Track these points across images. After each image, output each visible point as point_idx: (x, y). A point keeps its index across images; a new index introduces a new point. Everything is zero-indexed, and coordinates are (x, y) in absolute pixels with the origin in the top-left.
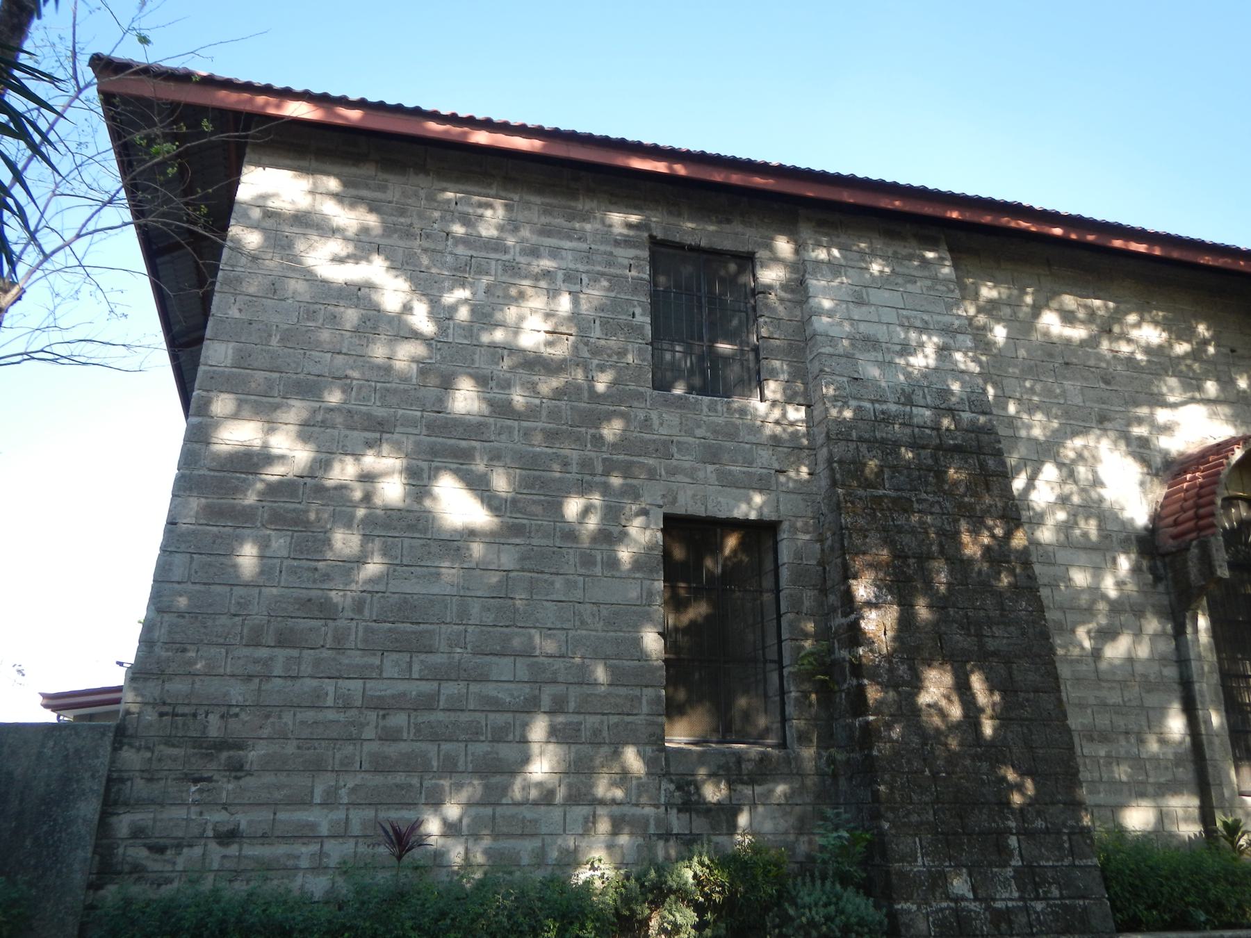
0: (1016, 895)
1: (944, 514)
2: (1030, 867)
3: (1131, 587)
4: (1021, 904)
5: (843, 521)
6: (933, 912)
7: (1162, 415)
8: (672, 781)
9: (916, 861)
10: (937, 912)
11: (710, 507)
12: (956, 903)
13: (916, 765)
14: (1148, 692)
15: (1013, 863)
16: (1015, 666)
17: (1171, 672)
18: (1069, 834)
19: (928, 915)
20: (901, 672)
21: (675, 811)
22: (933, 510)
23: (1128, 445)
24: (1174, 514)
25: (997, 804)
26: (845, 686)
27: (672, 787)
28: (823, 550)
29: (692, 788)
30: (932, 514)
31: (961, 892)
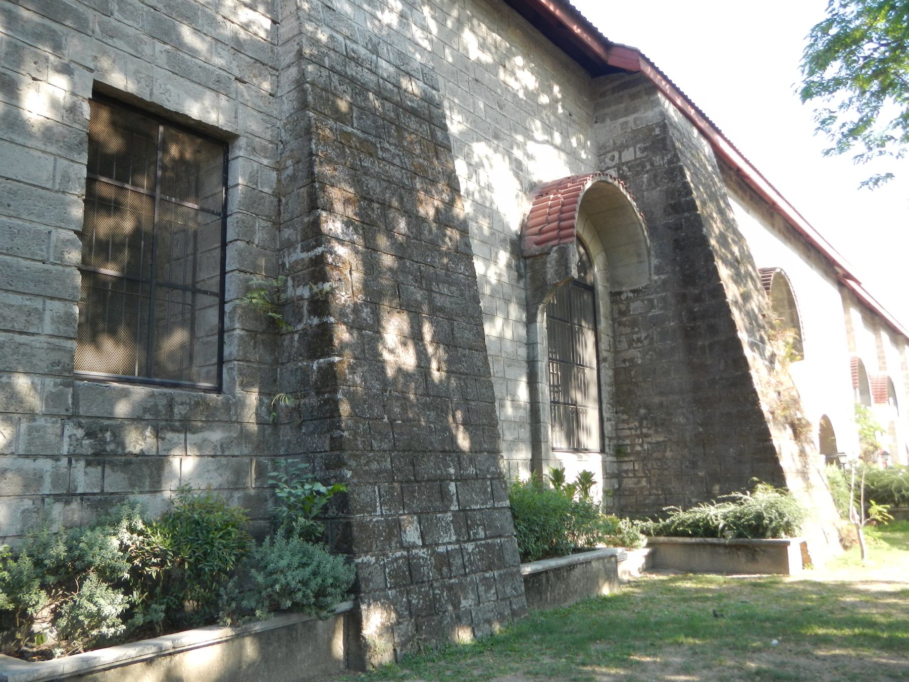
0: (454, 538)
1: (403, 168)
2: (464, 510)
3: (505, 279)
4: (457, 546)
5: (313, 146)
6: (389, 563)
7: (531, 146)
8: (80, 425)
9: (375, 511)
10: (392, 562)
11: (155, 92)
12: (408, 552)
13: (377, 411)
14: (509, 366)
15: (452, 508)
16: (455, 323)
17: (523, 352)
18: (491, 479)
19: (384, 566)
20: (364, 315)
21: (82, 463)
22: (395, 161)
23: (511, 163)
24: (540, 225)
25: (441, 452)
26: (300, 327)
27: (80, 433)
28: (279, 181)
29: (108, 435)
30: (394, 165)
31: (412, 540)
